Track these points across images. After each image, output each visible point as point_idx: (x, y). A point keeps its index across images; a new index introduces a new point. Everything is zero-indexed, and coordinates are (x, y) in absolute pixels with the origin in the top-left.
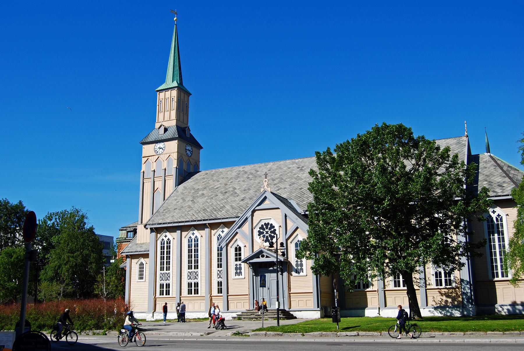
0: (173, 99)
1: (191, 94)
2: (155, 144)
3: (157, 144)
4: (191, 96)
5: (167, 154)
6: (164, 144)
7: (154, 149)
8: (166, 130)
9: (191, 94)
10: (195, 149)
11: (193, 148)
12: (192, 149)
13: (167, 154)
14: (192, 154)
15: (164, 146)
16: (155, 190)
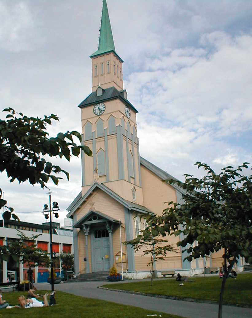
0: (108, 62)
1: (123, 62)
2: (94, 106)
3: (96, 106)
4: (123, 63)
5: (107, 114)
6: (104, 105)
7: (94, 110)
8: (104, 91)
9: (123, 62)
10: (132, 113)
11: (131, 111)
12: (130, 111)
13: (107, 114)
14: (130, 116)
15: (104, 107)
16: (97, 152)
